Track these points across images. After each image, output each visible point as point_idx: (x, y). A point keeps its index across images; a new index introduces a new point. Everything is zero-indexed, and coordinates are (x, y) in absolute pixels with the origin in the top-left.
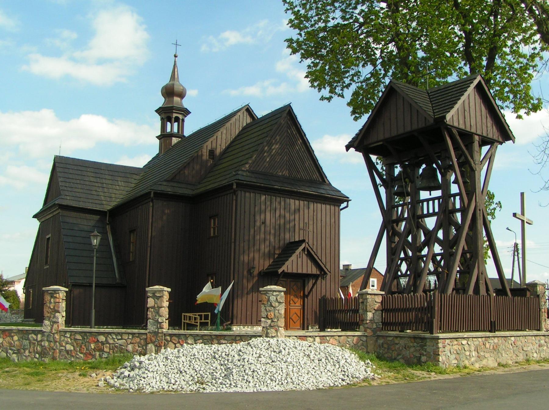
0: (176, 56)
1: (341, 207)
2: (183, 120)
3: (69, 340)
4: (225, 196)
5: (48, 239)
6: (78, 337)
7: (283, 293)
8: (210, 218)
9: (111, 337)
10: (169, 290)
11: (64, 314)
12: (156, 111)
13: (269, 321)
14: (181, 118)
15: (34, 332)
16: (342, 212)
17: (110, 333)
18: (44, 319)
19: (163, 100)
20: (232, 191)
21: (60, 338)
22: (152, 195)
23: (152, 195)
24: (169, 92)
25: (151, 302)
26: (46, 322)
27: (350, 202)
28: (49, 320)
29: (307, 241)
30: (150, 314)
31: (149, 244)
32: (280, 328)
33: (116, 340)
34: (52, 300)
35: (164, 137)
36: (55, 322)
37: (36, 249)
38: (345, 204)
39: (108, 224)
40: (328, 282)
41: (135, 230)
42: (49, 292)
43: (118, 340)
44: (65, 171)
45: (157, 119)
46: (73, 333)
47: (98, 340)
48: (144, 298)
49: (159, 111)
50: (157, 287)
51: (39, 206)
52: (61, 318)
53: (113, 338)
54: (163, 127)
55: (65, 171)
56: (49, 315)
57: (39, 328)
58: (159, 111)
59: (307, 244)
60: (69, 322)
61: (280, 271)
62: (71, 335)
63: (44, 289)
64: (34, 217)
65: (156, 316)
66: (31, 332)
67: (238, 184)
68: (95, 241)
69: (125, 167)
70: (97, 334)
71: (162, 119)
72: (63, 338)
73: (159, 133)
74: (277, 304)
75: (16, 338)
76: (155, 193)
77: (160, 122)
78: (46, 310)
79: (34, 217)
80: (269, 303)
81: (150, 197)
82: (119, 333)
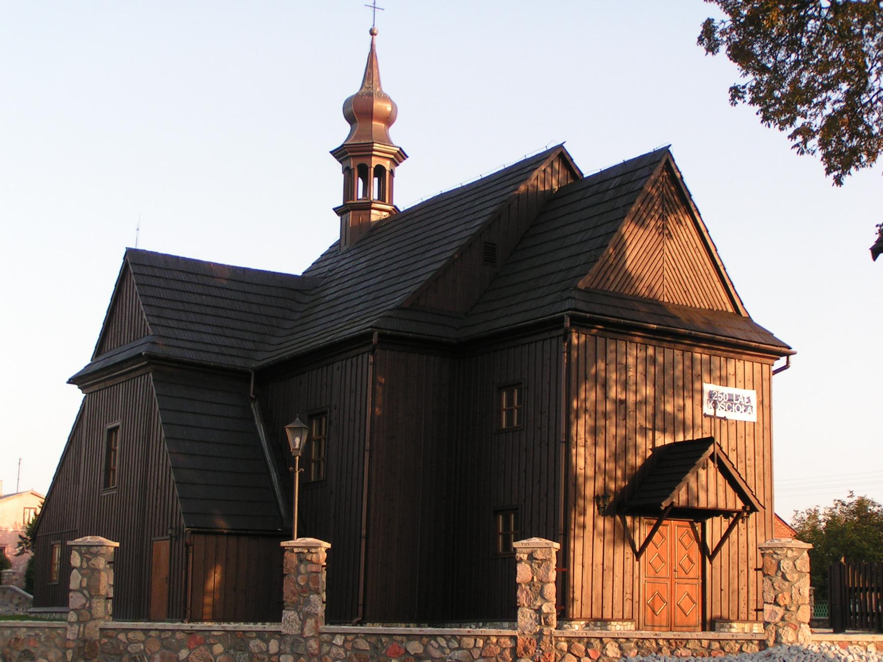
0: (372, 33)
1: (774, 368)
2: (392, 173)
3: (341, 651)
4: (539, 344)
5: (115, 430)
6: (363, 644)
7: (805, 554)
8: (500, 389)
9: (436, 646)
10: (329, 545)
11: (324, 596)
12: (331, 152)
13: (780, 611)
14: (388, 168)
15: (260, 635)
16: (775, 378)
17: (434, 637)
18: (284, 608)
19: (346, 128)
20: (561, 332)
21: (320, 647)
22: (375, 339)
23: (375, 339)
24: (362, 111)
25: (523, 572)
26: (289, 615)
27: (791, 357)
28: (296, 609)
29: (717, 440)
30: (522, 597)
31: (368, 445)
32: (802, 625)
33: (448, 651)
34: (302, 568)
35: (350, 209)
36: (308, 615)
37: (72, 455)
38: (782, 361)
39: (254, 400)
40: (752, 531)
41: (325, 413)
42: (296, 550)
43: (452, 650)
44: (150, 284)
45: (336, 169)
46: (350, 638)
47: (407, 652)
48: (512, 562)
49: (339, 154)
50: (535, 540)
51: (82, 357)
52: (318, 604)
53: (441, 648)
54: (349, 189)
55: (150, 284)
56: (294, 599)
57: (269, 627)
58: (339, 154)
59: (717, 447)
60: (334, 615)
61: (665, 504)
62: (345, 641)
63: (283, 544)
64: (72, 381)
65: (536, 599)
66: (254, 635)
67: (573, 318)
68: (297, 440)
69: (274, 274)
70: (404, 638)
71: (347, 171)
72: (325, 648)
73: (340, 202)
74: (796, 576)
75: (218, 648)
76: (380, 335)
77: (343, 175)
78: (288, 588)
79: (72, 381)
80: (780, 574)
81: (371, 342)
82: (454, 636)
